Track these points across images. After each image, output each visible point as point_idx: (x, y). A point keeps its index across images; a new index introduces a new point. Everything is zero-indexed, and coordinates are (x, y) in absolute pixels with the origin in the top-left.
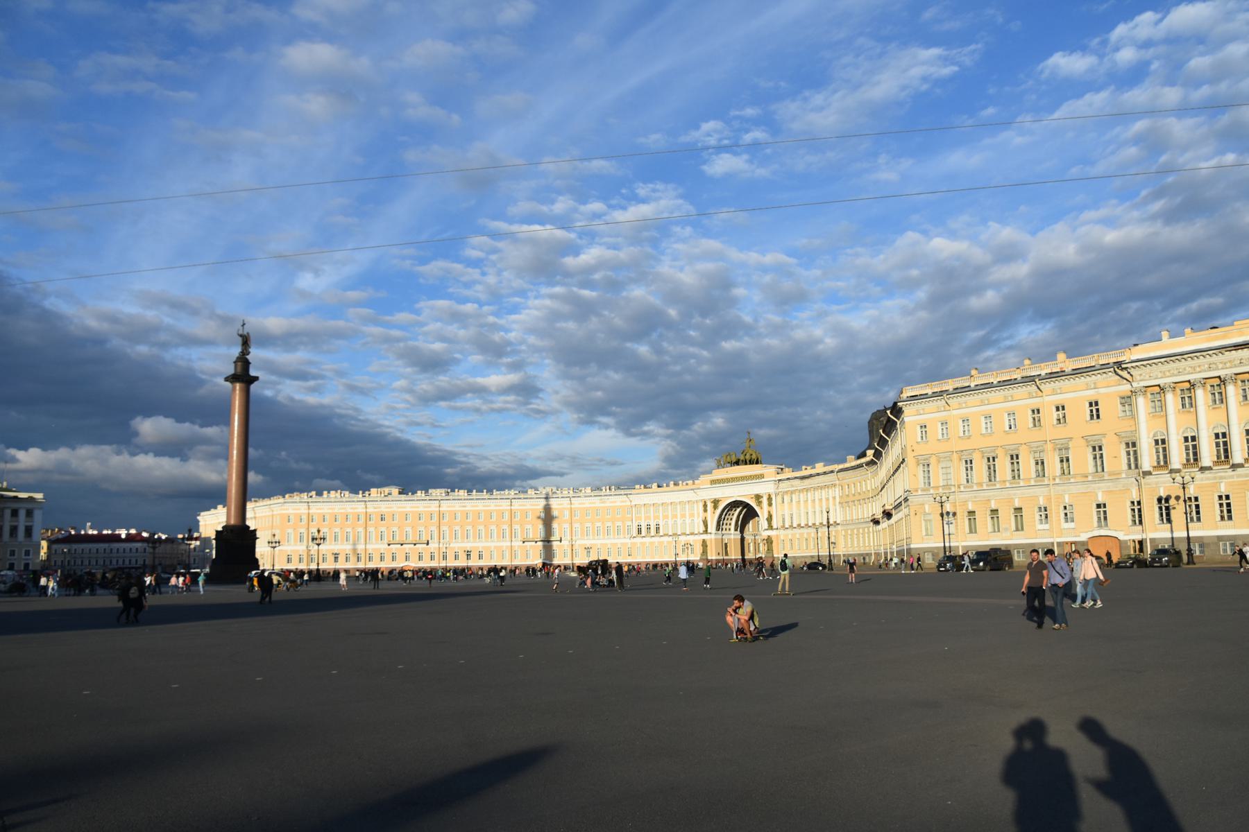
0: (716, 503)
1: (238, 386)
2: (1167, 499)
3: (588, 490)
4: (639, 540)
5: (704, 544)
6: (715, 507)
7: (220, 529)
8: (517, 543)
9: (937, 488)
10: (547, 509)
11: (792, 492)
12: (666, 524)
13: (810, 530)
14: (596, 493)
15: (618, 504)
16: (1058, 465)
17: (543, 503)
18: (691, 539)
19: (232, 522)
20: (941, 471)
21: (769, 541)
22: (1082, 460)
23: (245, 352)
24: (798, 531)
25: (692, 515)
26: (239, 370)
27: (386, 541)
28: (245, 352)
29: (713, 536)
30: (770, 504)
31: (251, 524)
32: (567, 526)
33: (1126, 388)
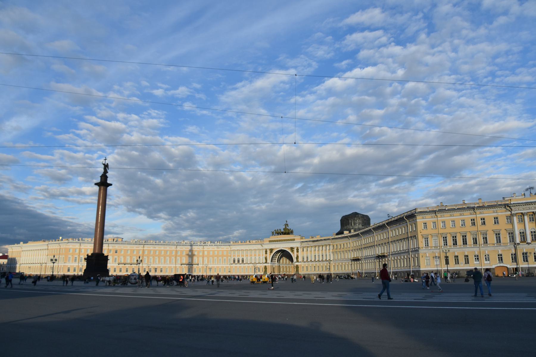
0: (271, 250)
1: (102, 188)
2: (526, 253)
3: (209, 243)
4: (234, 265)
5: (266, 268)
6: (271, 252)
7: (90, 255)
8: (178, 266)
9: (432, 247)
10: (191, 251)
11: (308, 247)
12: (247, 258)
13: (328, 262)
14: (236, 244)
15: (225, 249)
16: (483, 240)
17: (189, 248)
18: (258, 265)
19: (97, 251)
20: (433, 241)
21: (297, 267)
22: (492, 239)
23: (106, 172)
24: (310, 263)
25: (259, 255)
26: (103, 180)
27: (117, 262)
28: (106, 172)
29: (270, 265)
30: (298, 252)
31: (105, 253)
32: (201, 259)
33: (509, 213)
